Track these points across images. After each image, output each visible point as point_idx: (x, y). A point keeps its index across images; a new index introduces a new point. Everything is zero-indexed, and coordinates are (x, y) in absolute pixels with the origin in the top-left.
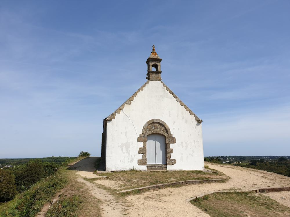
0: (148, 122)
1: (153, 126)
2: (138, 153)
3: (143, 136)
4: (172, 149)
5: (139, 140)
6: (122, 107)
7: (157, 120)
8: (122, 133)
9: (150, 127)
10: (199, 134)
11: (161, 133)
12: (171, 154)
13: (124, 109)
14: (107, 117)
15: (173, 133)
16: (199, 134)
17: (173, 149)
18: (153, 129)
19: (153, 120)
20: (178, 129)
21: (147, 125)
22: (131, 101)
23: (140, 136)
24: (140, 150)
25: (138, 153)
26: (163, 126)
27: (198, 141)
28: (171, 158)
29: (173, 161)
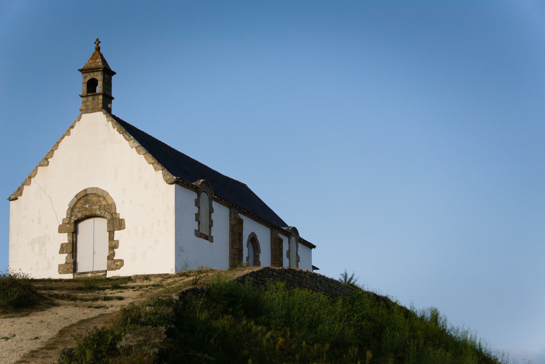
0: (76, 196)
1: (87, 202)
2: (60, 253)
3: (67, 222)
4: (118, 241)
5: (61, 230)
6: (33, 174)
7: (93, 189)
8: (33, 220)
9: (81, 205)
10: (168, 208)
11: (99, 213)
12: (115, 250)
13: (36, 176)
14: (12, 195)
15: (122, 211)
16: (168, 208)
17: (119, 241)
18: (85, 207)
19: (85, 190)
20: (131, 201)
21: (76, 200)
22: (49, 160)
23: (63, 224)
24: (62, 247)
25: (60, 253)
26: (104, 199)
27: (166, 222)
28: (115, 258)
29: (119, 263)
